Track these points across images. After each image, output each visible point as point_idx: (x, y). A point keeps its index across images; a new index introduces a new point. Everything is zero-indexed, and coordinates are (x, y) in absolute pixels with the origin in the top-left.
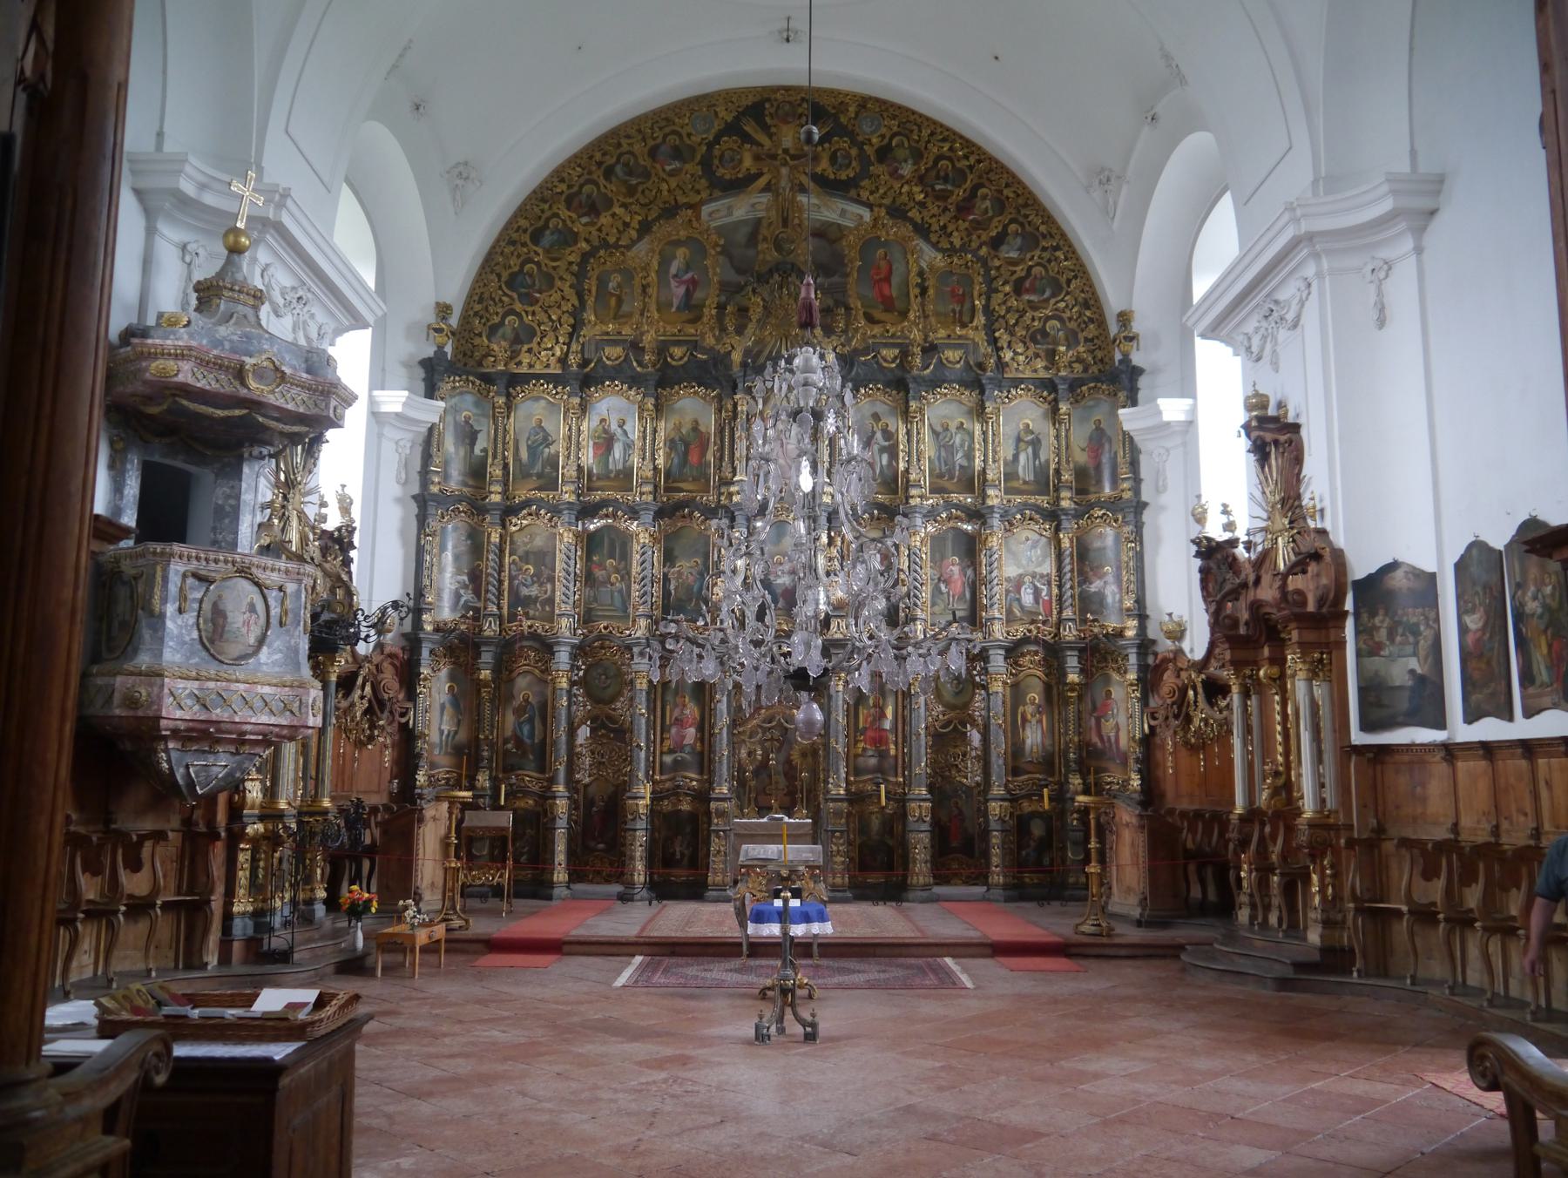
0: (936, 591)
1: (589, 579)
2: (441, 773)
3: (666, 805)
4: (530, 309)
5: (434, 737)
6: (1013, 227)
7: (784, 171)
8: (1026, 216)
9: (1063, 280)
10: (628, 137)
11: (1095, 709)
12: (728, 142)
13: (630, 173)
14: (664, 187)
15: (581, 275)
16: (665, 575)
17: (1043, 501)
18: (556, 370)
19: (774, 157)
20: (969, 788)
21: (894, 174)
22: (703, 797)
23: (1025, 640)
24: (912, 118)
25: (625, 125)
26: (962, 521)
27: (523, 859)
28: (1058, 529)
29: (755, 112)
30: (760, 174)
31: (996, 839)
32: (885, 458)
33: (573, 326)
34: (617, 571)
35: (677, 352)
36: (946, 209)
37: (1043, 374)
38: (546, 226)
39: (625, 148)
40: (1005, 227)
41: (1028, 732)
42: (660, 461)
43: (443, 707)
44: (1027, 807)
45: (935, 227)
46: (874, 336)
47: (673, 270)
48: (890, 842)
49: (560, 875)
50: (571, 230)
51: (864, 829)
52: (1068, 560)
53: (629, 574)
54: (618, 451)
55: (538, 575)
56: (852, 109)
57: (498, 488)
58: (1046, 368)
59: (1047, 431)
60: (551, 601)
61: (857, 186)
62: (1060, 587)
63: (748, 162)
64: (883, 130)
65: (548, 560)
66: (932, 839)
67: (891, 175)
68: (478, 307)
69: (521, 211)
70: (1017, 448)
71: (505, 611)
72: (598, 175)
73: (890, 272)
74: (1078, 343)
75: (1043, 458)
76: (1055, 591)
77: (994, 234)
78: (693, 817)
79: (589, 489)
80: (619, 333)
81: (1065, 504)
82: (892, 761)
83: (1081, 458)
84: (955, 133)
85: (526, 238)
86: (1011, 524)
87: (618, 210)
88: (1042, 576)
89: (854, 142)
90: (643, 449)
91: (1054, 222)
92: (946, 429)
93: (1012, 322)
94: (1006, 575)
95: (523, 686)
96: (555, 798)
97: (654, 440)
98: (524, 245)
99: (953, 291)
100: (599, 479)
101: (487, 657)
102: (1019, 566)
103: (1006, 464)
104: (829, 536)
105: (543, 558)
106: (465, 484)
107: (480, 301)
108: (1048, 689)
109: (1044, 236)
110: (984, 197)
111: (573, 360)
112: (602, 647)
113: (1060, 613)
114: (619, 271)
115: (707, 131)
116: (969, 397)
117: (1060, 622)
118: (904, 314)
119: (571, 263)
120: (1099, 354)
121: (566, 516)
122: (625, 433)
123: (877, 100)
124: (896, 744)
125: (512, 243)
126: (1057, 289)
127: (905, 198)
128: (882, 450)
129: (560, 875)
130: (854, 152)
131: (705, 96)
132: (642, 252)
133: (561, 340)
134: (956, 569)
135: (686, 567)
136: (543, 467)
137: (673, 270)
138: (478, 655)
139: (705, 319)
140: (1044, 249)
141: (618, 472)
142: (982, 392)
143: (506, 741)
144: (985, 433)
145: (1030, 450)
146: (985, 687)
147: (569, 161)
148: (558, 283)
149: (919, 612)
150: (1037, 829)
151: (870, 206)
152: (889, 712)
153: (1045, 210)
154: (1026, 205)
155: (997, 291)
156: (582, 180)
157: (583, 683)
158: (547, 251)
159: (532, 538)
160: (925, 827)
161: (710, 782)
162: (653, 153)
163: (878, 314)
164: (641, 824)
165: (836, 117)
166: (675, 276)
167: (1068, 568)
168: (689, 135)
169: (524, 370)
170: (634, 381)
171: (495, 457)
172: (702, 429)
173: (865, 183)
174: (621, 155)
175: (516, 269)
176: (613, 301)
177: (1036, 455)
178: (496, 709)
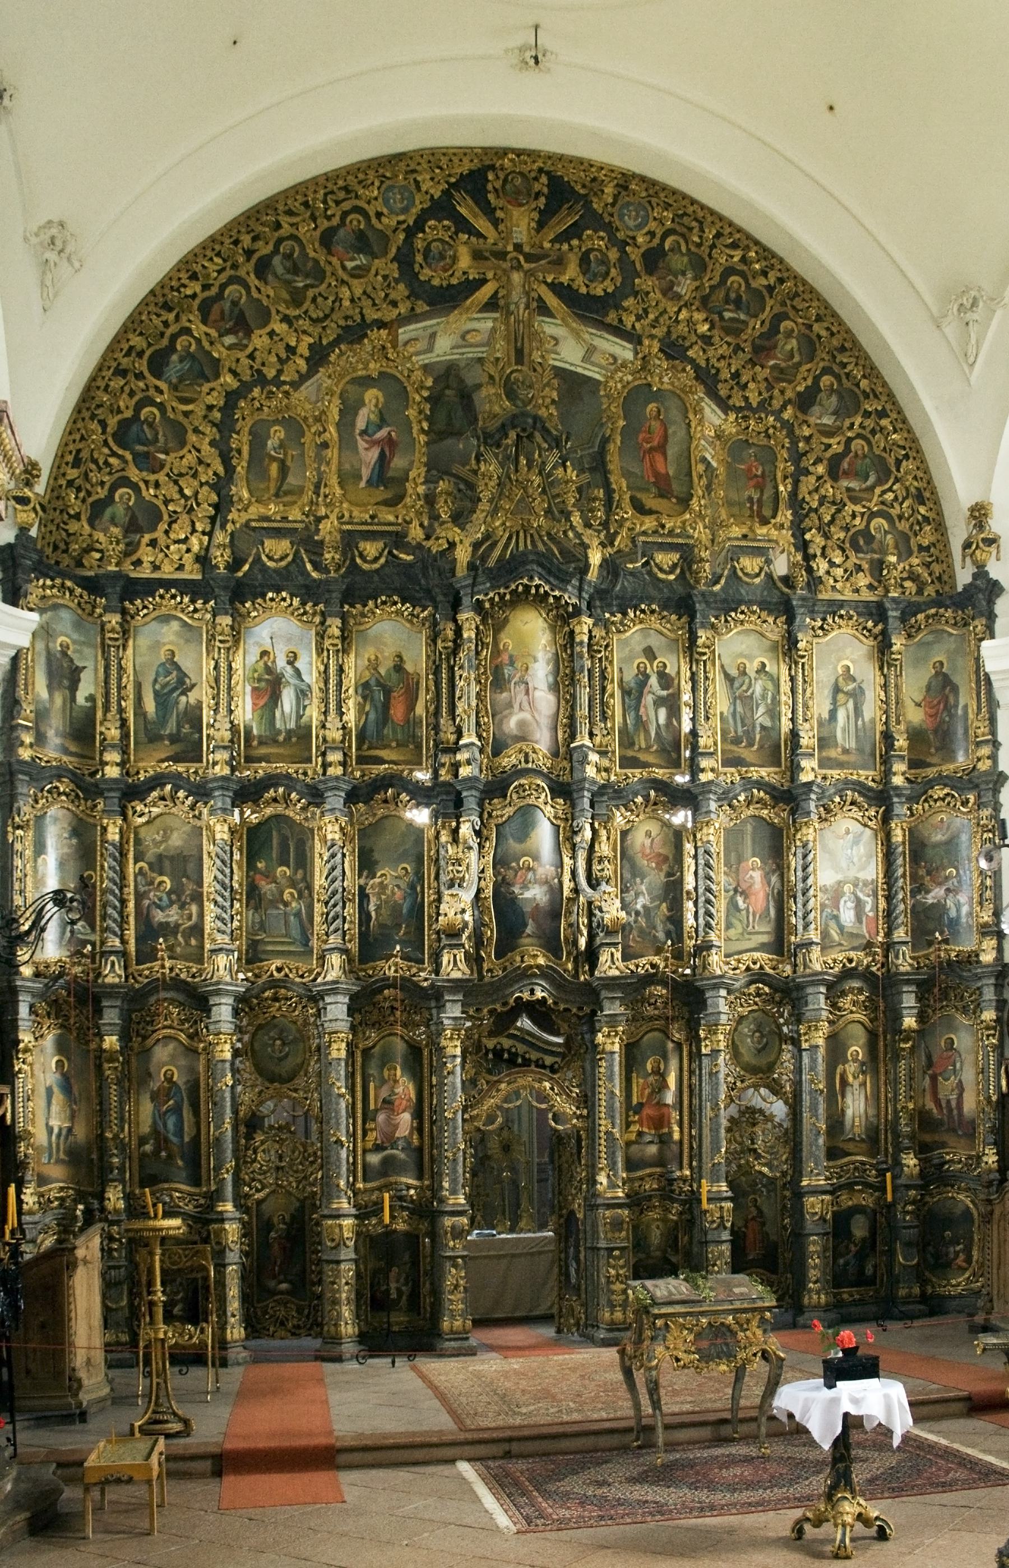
0: (733, 905)
1: (253, 895)
2: (53, 1190)
4: (152, 478)
5: (41, 1137)
6: (826, 380)
7: (517, 277)
8: (844, 365)
9: (891, 461)
10: (290, 213)
11: (930, 1064)
12: (436, 229)
13: (295, 270)
14: (345, 293)
15: (226, 427)
17: (867, 776)
18: (192, 573)
19: (502, 255)
20: (772, 1181)
21: (668, 291)
23: (847, 974)
24: (690, 210)
25: (285, 193)
26: (765, 806)
27: (176, 1310)
28: (886, 819)
29: (476, 181)
30: (483, 281)
31: (814, 1245)
32: (663, 713)
33: (216, 507)
34: (293, 884)
35: (371, 548)
36: (738, 348)
37: (867, 596)
38: (171, 348)
39: (286, 230)
40: (817, 379)
41: (849, 1100)
43: (49, 1092)
44: (847, 1201)
45: (725, 374)
46: (644, 533)
47: (361, 424)
50: (209, 353)
52: (900, 861)
53: (310, 887)
54: (288, 699)
55: (177, 891)
56: (609, 190)
57: (113, 756)
58: (870, 587)
59: (868, 674)
60: (198, 930)
61: (618, 307)
62: (889, 898)
63: (465, 262)
64: (652, 225)
65: (191, 866)
67: (664, 293)
68: (72, 473)
69: (133, 324)
70: (834, 701)
71: (132, 947)
72: (247, 270)
73: (665, 437)
74: (910, 554)
76: (882, 904)
77: (800, 388)
78: (412, 1239)
79: (249, 759)
80: (285, 519)
81: (898, 780)
82: (675, 1148)
83: (915, 716)
84: (748, 236)
85: (142, 365)
86: (828, 810)
87: (280, 328)
88: (866, 884)
89: (613, 240)
91: (879, 376)
92: (744, 673)
93: (827, 518)
94: (821, 883)
95: (165, 1060)
96: (222, 1221)
97: (340, 684)
98: (140, 376)
99: (749, 470)
101: (111, 1016)
102: (837, 869)
103: (820, 724)
105: (184, 866)
106: (66, 751)
107: (77, 463)
108: (873, 1037)
109: (867, 396)
110: (789, 334)
111: (220, 558)
112: (275, 999)
113: (888, 934)
114: (283, 422)
115: (405, 210)
116: (774, 629)
117: (888, 947)
118: (684, 502)
119: (210, 408)
120: (937, 568)
121: (219, 800)
122: (298, 673)
123: (643, 179)
124: (681, 1126)
125: (121, 372)
126: (884, 474)
127: (682, 329)
128: (659, 702)
130: (613, 255)
131: (400, 157)
132: (317, 397)
133: (199, 527)
134: (757, 875)
135: (391, 877)
136: (179, 726)
137: (361, 424)
138: (99, 1012)
139: (408, 500)
140: (867, 414)
141: (289, 733)
142: (790, 621)
143: (142, 1141)
144: (792, 679)
145: (851, 705)
146: (796, 1042)
147: (203, 246)
148: (192, 438)
150: (859, 1229)
151: (634, 338)
152: (672, 1080)
153: (867, 358)
154: (843, 349)
155: (807, 473)
156: (223, 278)
158: (175, 388)
159: (166, 838)
160: (726, 1236)
161: (435, 1189)
162: (327, 240)
163: (650, 502)
164: (348, 1253)
165: (588, 204)
166: (364, 433)
167: (900, 871)
168: (379, 215)
169: (145, 572)
170: (310, 592)
171: (107, 709)
172: (409, 667)
173: (629, 302)
174: (280, 241)
175: (128, 414)
176: (274, 469)
177: (858, 711)
178: (125, 1094)
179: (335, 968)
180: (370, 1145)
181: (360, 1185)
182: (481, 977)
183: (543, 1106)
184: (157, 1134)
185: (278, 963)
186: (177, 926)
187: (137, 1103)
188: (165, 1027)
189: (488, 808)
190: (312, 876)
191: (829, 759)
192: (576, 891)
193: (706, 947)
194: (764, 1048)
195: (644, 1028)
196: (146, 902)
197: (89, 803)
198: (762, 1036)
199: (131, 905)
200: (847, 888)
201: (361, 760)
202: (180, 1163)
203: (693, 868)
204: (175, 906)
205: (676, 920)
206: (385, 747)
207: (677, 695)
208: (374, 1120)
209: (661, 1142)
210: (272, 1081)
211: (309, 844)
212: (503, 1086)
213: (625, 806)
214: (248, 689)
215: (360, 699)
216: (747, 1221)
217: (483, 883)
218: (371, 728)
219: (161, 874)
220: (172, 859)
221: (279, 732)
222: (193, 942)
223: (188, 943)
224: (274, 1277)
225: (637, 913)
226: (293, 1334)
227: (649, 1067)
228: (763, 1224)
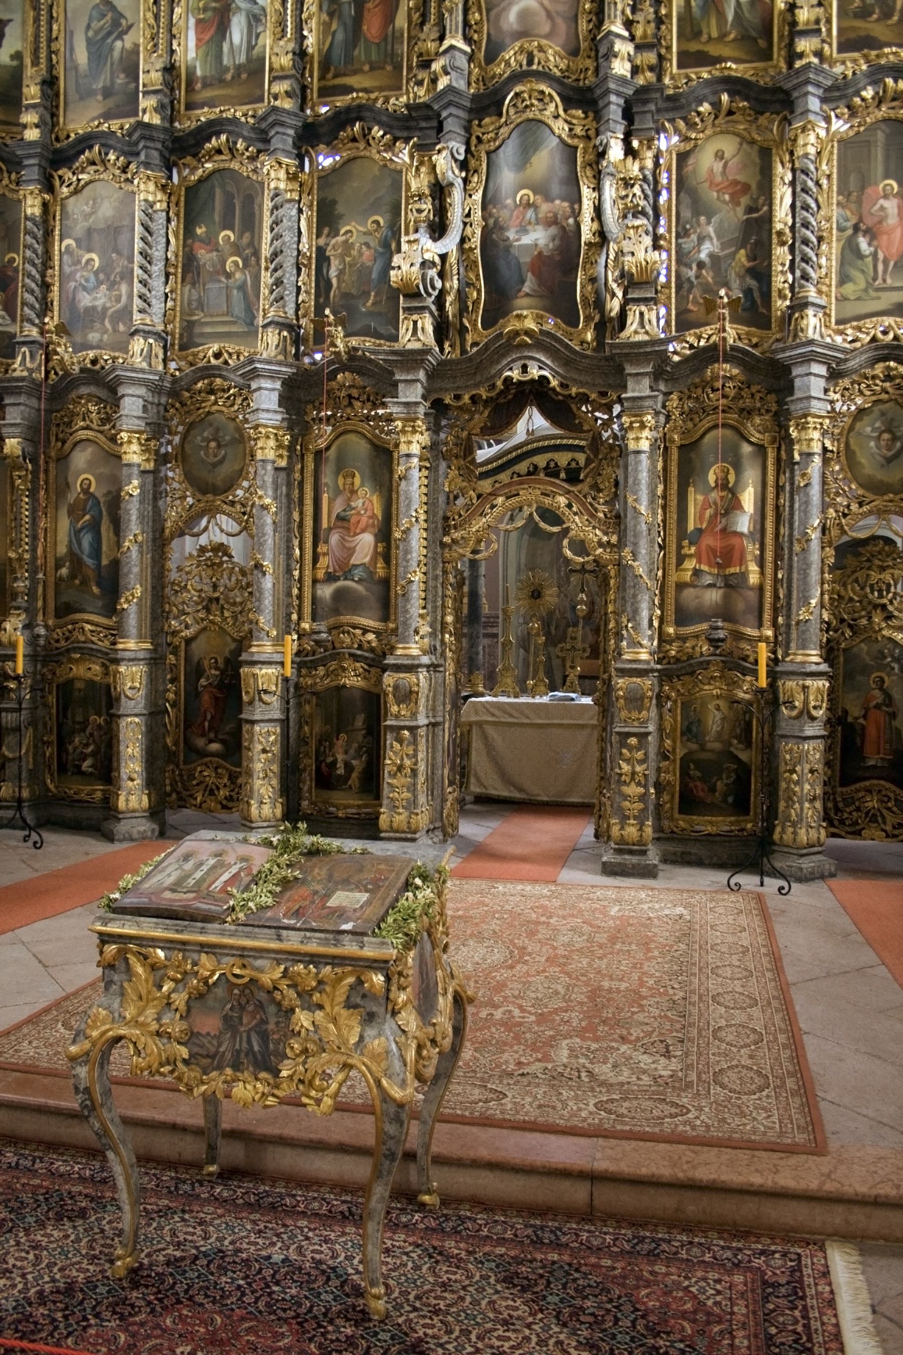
0: (850, 251)
1: (189, 269)
3: (319, 678)
16: (321, 251)
22: (377, 662)
27: (86, 765)
34: (237, 250)
42: (311, 41)
48: (743, 756)
49: (133, 795)
51: (691, 729)
53: (257, 253)
54: (237, 32)
66: (829, 749)
79: (189, 106)
82: (752, 596)
90: (281, 23)
100: (205, 85)
104: (627, 142)
124: (761, 564)
129: (133, 795)
135: (357, 232)
141: (239, 68)
149: (811, 293)
152: (748, 499)
157: (181, 456)
179: (269, 343)
180: (321, 574)
181: (306, 626)
182: (463, 351)
183: (555, 529)
184: (74, 558)
185: (216, 347)
186: (105, 309)
187: (56, 520)
188: (83, 428)
189: (478, 132)
192: (602, 237)
193: (799, 305)
194: (896, 456)
195: (706, 423)
196: (72, 284)
197: (13, 176)
198: (894, 439)
199: (56, 289)
201: (326, 92)
202: (95, 590)
203: (788, 200)
204: (104, 287)
205: (761, 274)
206: (355, 72)
208: (326, 542)
209: (728, 586)
210: (204, 493)
211: (257, 201)
212: (500, 500)
213: (684, 119)
214: (192, 22)
215: (325, 17)
216: (867, 710)
217: (469, 230)
218: (337, 52)
219: (89, 251)
221: (227, 69)
222: (121, 328)
223: (115, 330)
224: (203, 735)
225: (701, 265)
226: (224, 807)
227: (711, 478)
228: (893, 716)
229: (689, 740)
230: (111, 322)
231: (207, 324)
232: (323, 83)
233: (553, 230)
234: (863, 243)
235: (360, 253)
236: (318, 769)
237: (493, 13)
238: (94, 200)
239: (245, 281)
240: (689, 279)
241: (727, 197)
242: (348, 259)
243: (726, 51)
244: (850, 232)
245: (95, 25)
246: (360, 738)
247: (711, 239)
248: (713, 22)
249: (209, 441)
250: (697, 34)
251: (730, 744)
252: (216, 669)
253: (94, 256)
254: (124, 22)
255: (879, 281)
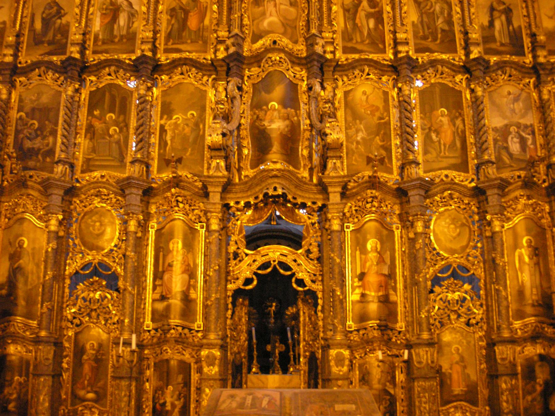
16: (162, 127)
54: (122, 20)
60: (51, 152)
65: (52, 114)
70: (491, 16)
75: (516, 24)
88: (526, 127)
100: (104, 43)
102: (505, 117)
128: (369, 16)
134: (445, 120)
136: (55, 35)
141: (122, 37)
145: (503, 18)
177: (509, 22)
186: (39, 150)
190: (129, 119)
191: (490, 49)
200: (513, 129)
204: (39, 138)
207: (380, 12)
208: (161, 278)
211: (130, 99)
219: (32, 119)
220: (40, 110)
221: (116, 37)
223: (44, 160)
224: (83, 388)
225: (358, 143)
228: (465, 367)
229: (363, 384)
230: (42, 156)
231: (97, 160)
232: (166, 47)
233: (287, 122)
234: (434, 136)
235: (184, 129)
236: (154, 408)
237: (255, 22)
238: (38, 94)
239: (119, 140)
240: (352, 149)
241: (369, 112)
242: (176, 131)
243: (365, 48)
244: (427, 131)
245: (47, 12)
246: (180, 388)
247: (362, 131)
248: (358, 35)
249: (95, 222)
250: (351, 40)
251: (386, 386)
252: (94, 350)
253: (35, 122)
254: (62, 11)
255: (442, 154)
